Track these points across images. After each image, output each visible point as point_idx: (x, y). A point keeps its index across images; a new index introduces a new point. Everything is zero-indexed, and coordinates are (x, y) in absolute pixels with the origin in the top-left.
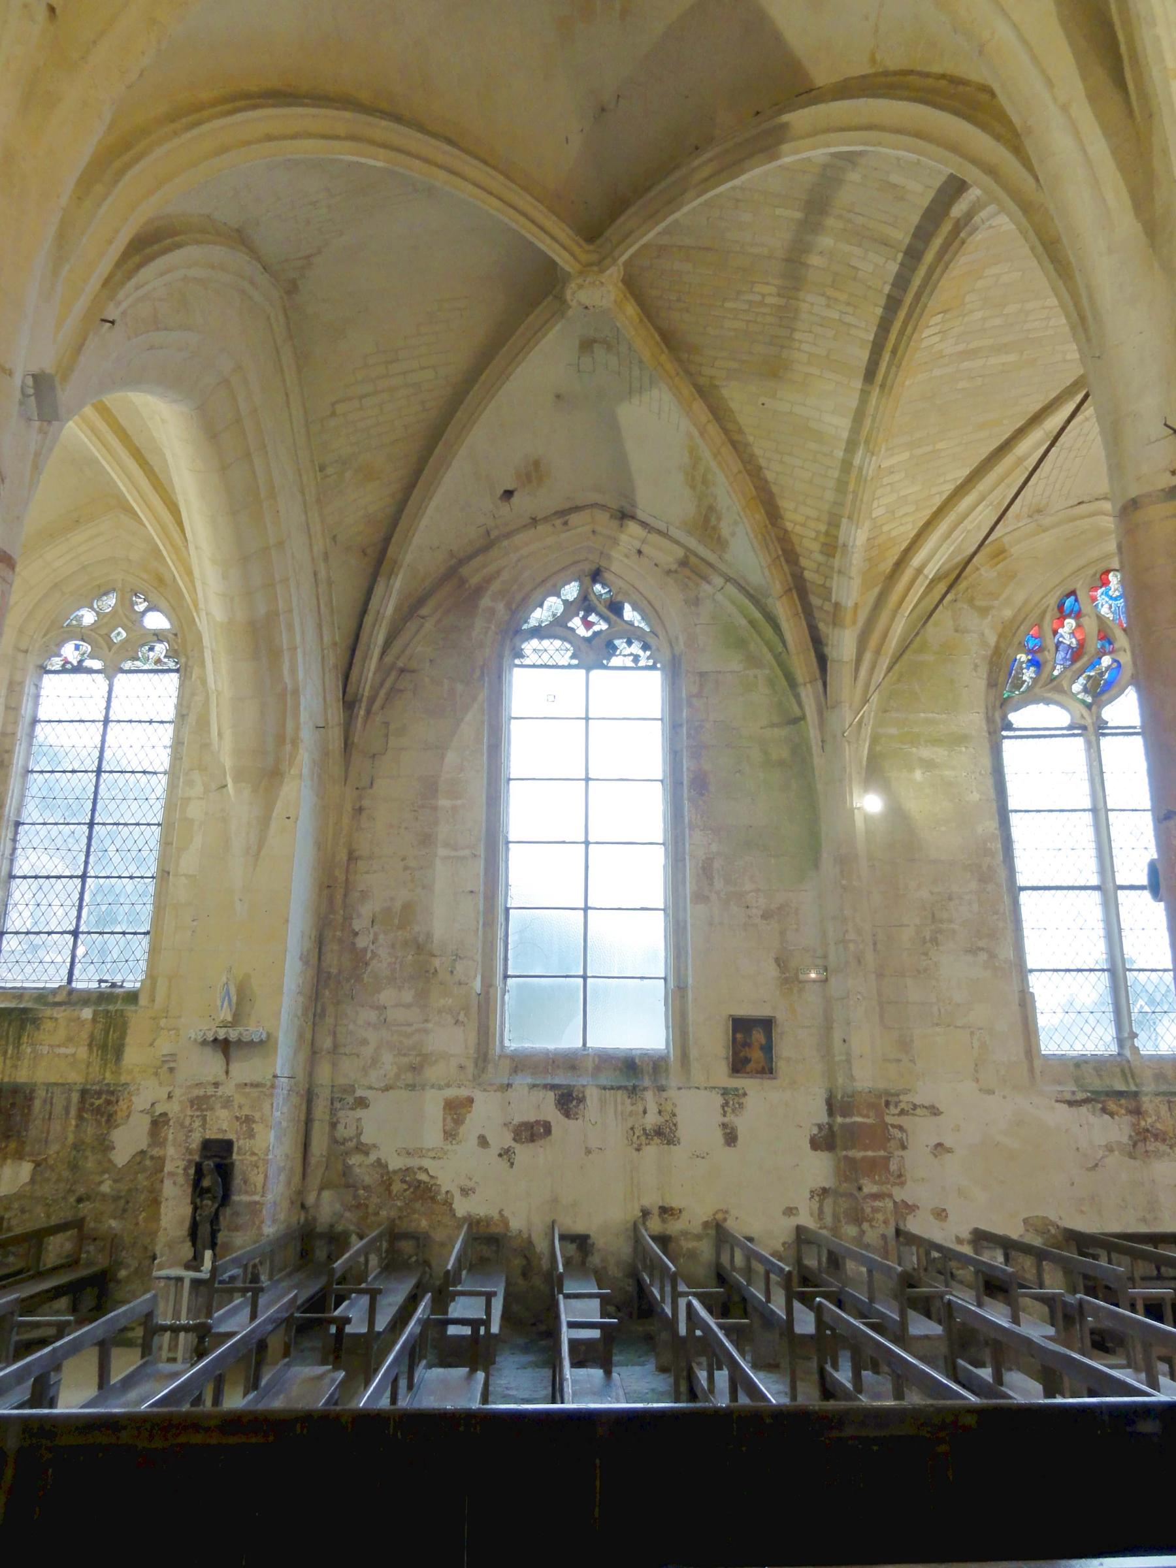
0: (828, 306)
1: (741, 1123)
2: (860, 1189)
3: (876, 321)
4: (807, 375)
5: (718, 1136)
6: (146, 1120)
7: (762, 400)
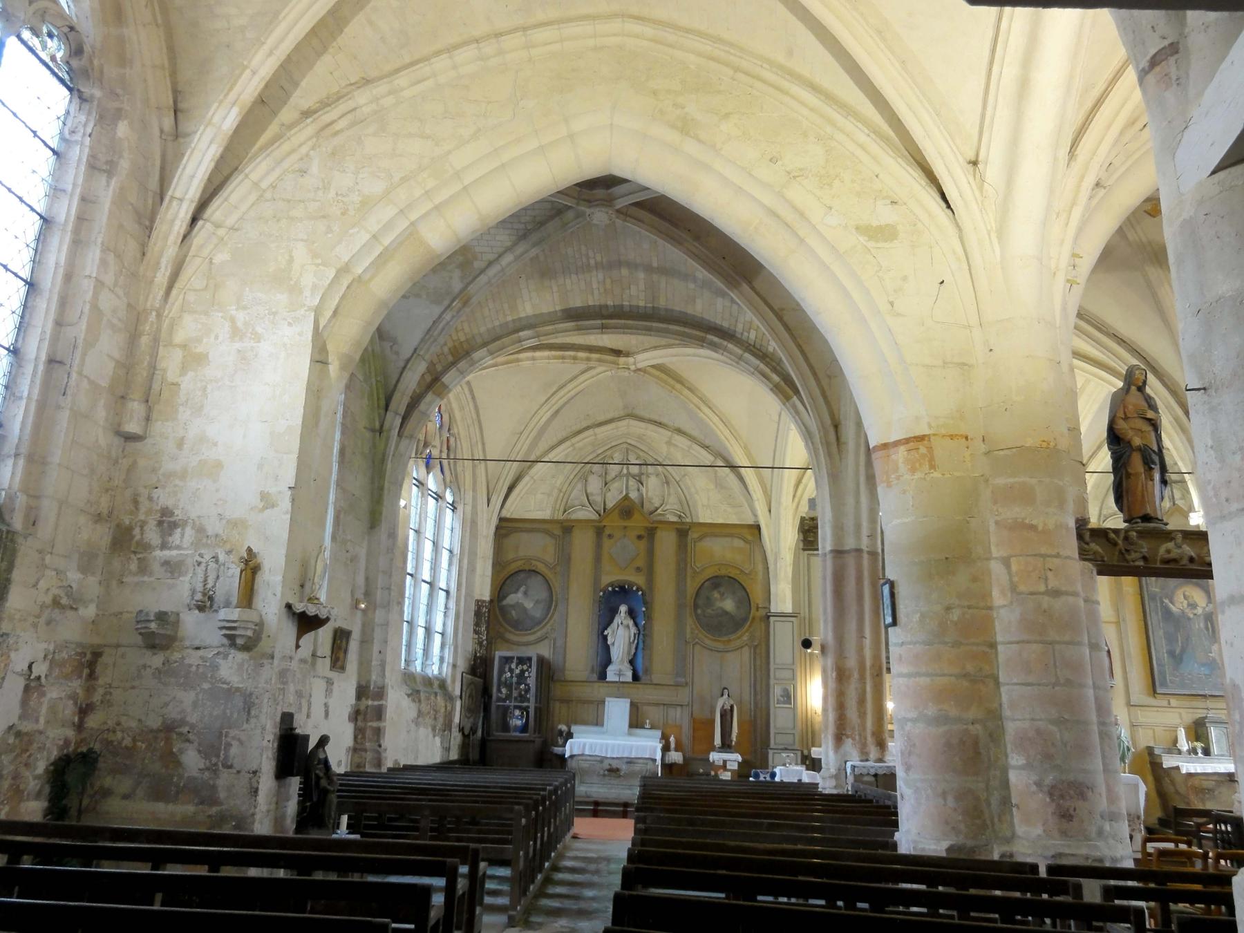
0: (599, 282)
1: (332, 702)
2: (380, 746)
3: (603, 302)
4: (551, 287)
5: (323, 714)
6: (21, 683)
7: (523, 276)
